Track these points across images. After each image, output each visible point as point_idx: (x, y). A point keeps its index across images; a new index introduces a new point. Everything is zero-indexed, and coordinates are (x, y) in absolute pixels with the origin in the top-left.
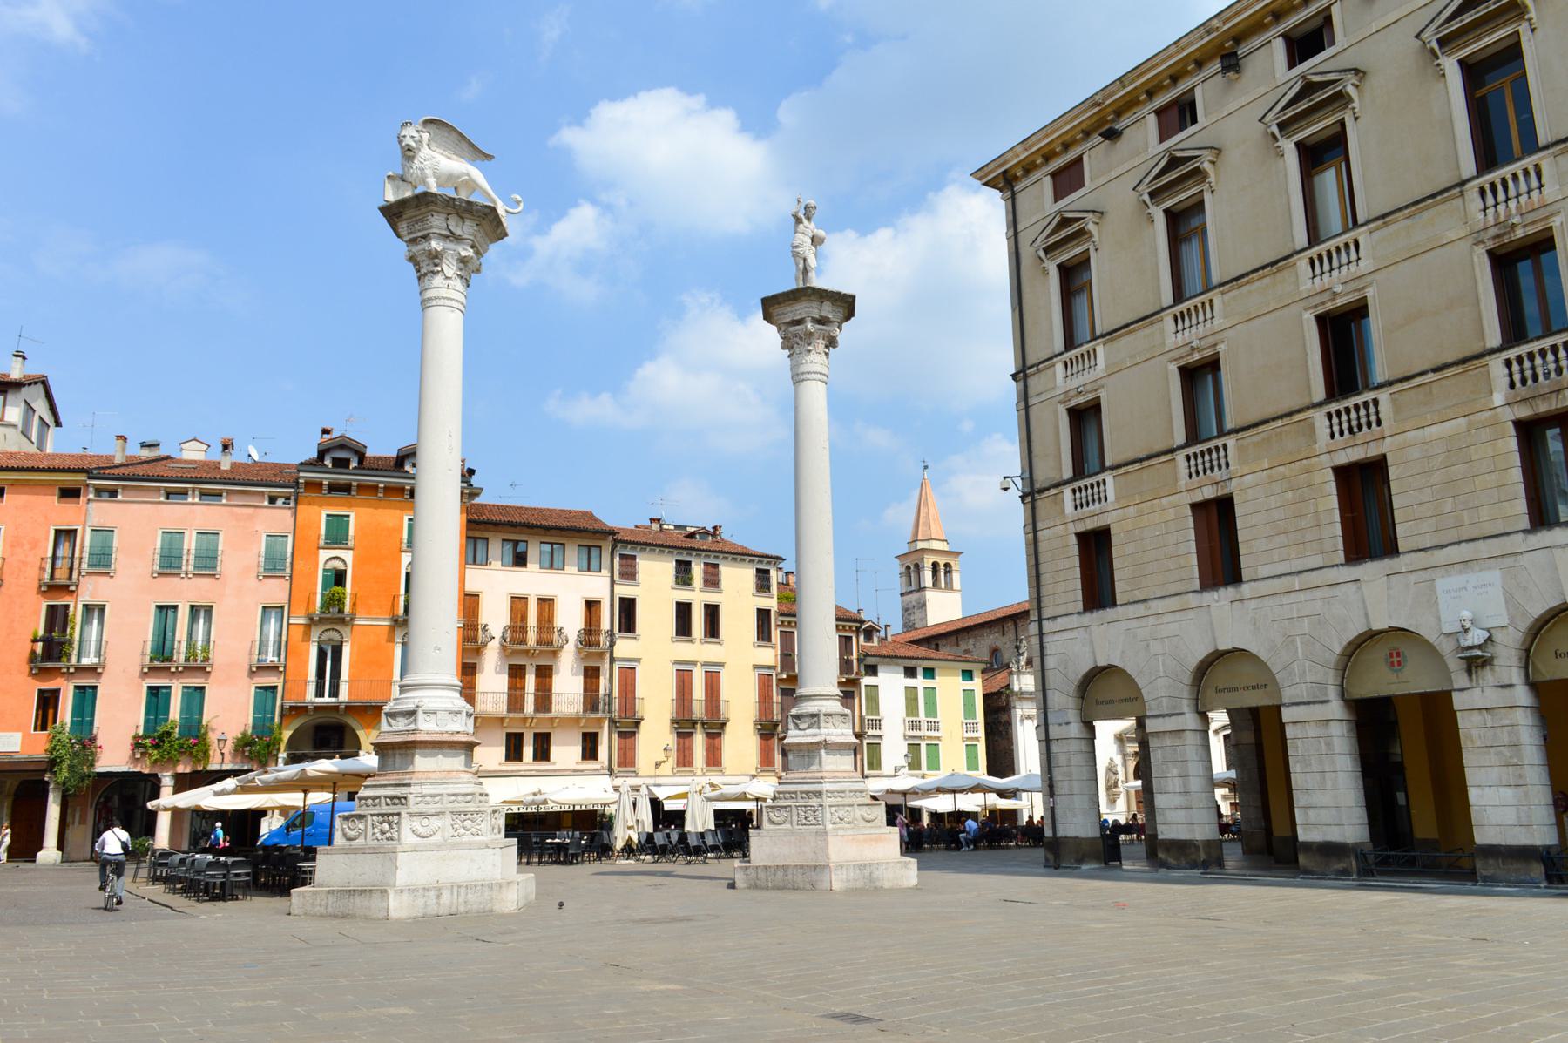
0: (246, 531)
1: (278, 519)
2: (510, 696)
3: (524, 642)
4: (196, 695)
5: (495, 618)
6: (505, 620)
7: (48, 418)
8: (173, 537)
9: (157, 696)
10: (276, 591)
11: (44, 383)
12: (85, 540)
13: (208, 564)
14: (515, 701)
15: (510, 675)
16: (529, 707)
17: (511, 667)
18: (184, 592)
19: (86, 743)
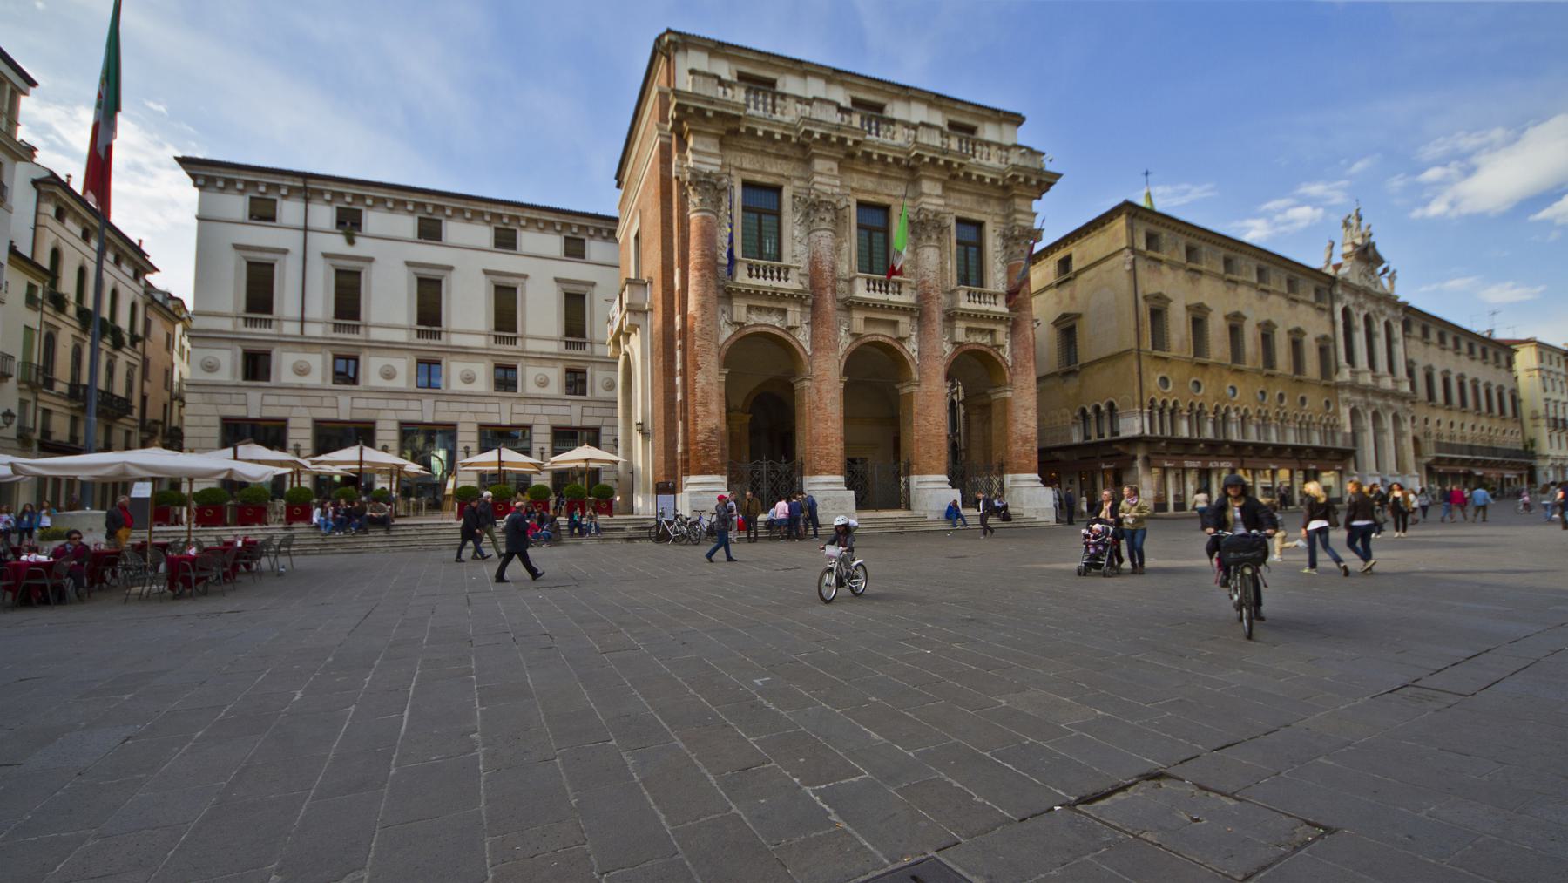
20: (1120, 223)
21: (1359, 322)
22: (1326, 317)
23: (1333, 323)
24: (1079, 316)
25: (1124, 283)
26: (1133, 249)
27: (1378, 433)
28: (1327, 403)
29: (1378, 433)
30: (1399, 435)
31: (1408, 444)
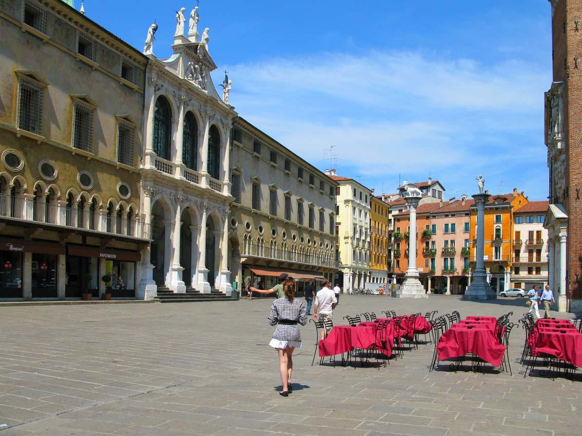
0: (460, 222)
1: (466, 219)
2: (529, 258)
3: (533, 243)
5: (524, 238)
6: (527, 238)
7: (441, 190)
8: (447, 225)
10: (467, 236)
11: (438, 182)
12: (431, 227)
13: (453, 230)
14: (530, 258)
15: (529, 253)
16: (534, 261)
17: (529, 250)
18: (449, 237)
19: (433, 271)
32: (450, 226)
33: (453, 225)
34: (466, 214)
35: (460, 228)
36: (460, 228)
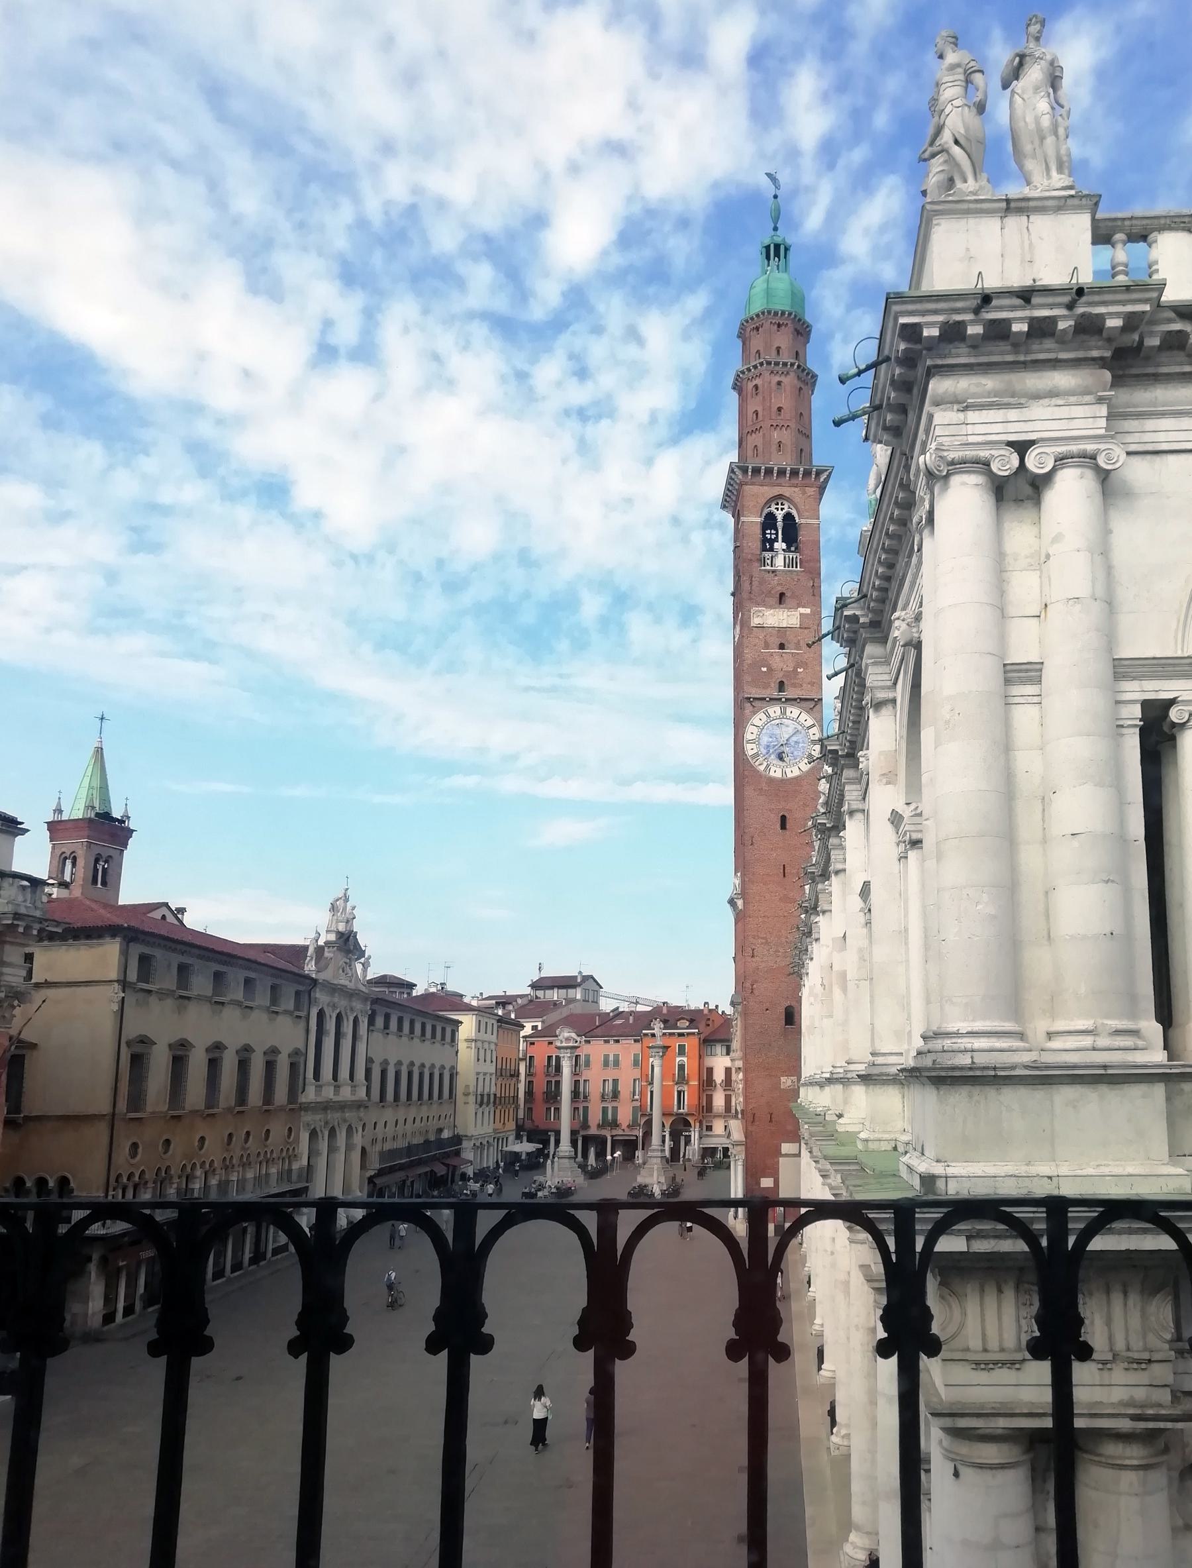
4: (615, 1109)
8: (606, 1057)
9: (605, 1110)
10: (637, 1073)
13: (617, 1063)
18: (611, 1074)
20: (111, 949)
21: (331, 1026)
22: (302, 1024)
23: (307, 1031)
24: (33, 1046)
25: (108, 1026)
26: (124, 984)
27: (332, 1149)
28: (290, 1129)
29: (332, 1149)
30: (349, 1147)
31: (356, 1156)
32: (611, 1058)
33: (616, 1057)
34: (635, 1041)
35: (626, 1061)
36: (626, 1061)
